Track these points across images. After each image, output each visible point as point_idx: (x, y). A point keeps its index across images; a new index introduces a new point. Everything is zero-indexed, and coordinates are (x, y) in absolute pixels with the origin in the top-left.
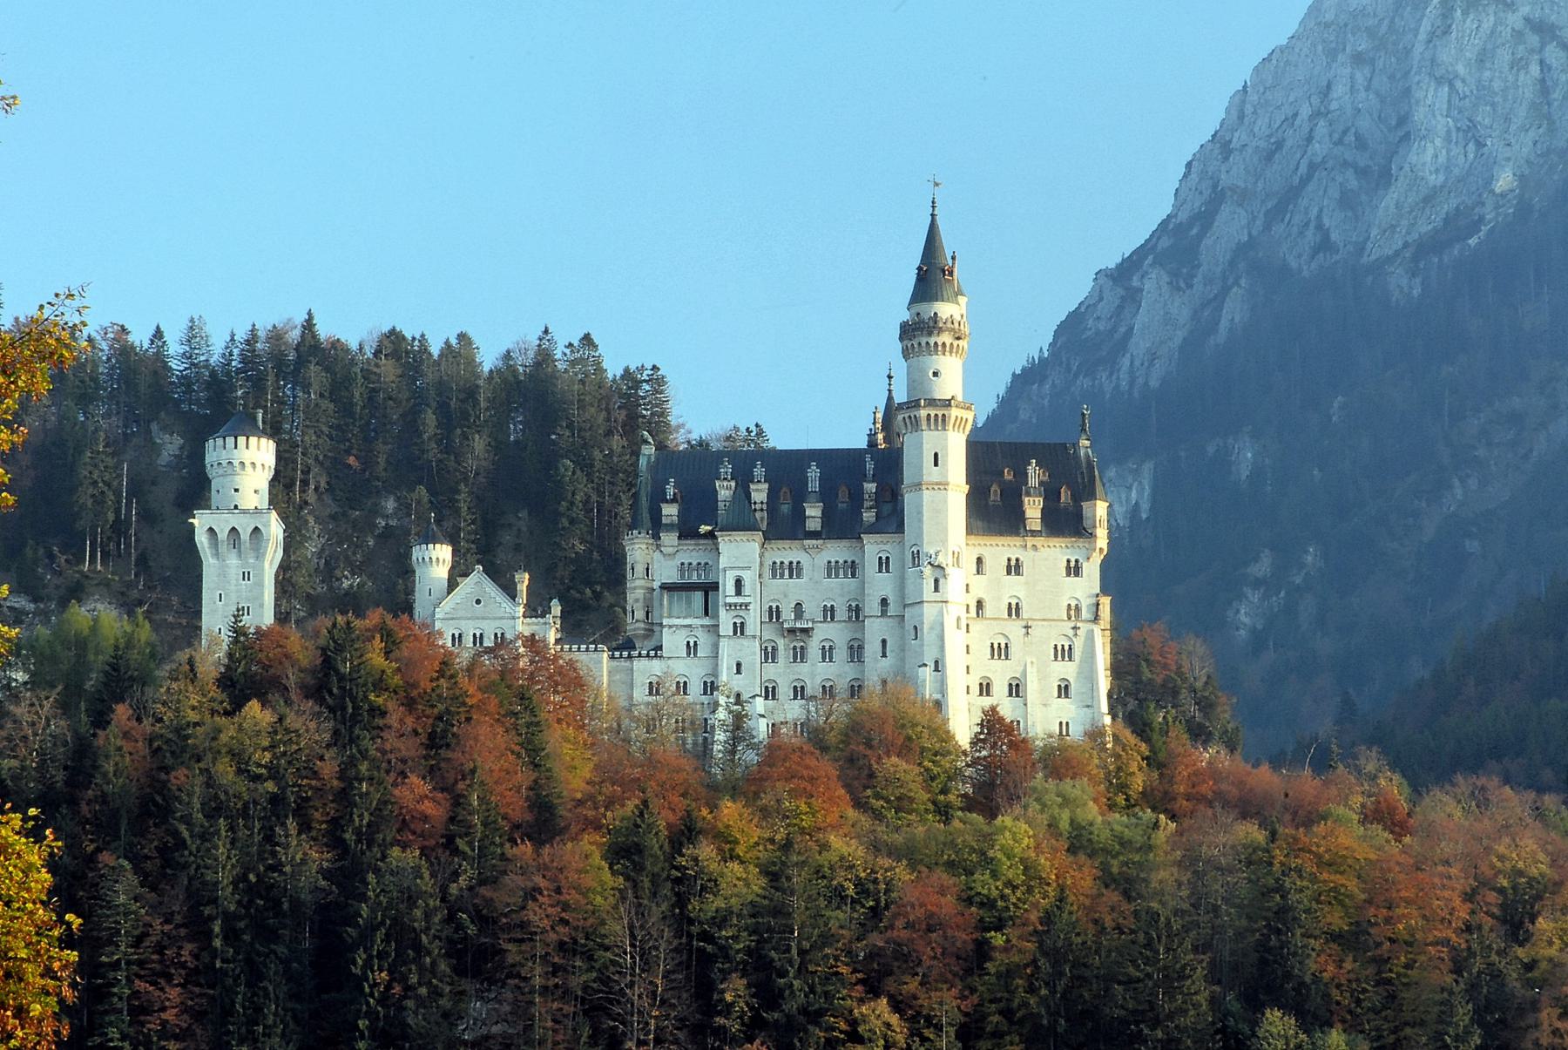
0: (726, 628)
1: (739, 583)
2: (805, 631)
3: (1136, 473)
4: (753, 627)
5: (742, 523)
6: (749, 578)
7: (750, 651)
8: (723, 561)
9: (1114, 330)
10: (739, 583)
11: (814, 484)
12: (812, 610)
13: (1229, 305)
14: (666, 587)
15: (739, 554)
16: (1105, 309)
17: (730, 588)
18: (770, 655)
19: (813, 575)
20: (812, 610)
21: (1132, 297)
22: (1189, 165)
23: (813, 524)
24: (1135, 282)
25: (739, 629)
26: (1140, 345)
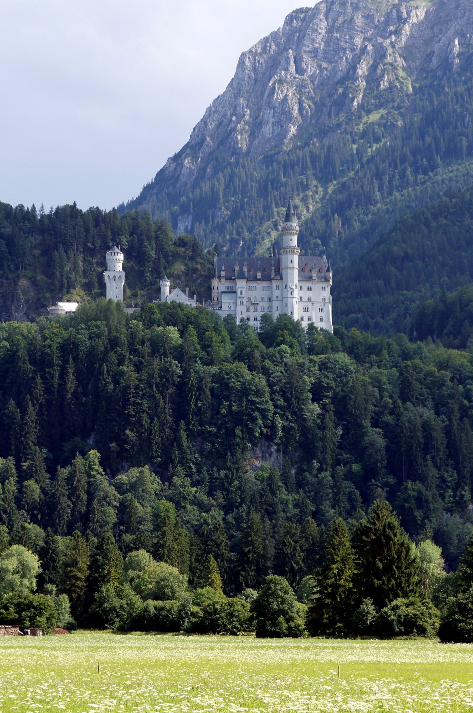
0: (238, 303)
1: (241, 292)
2: (257, 304)
3: (187, 218)
4: (244, 303)
5: (241, 276)
6: (244, 290)
7: (244, 308)
8: (238, 286)
9: (173, 175)
10: (241, 292)
11: (259, 267)
12: (259, 299)
13: (208, 170)
14: (223, 292)
15: (241, 284)
16: (171, 169)
17: (239, 293)
18: (248, 310)
19: (258, 290)
20: (259, 299)
21: (181, 165)
22: (194, 128)
23: (259, 277)
24: (180, 162)
25: (242, 303)
26: (183, 179)
